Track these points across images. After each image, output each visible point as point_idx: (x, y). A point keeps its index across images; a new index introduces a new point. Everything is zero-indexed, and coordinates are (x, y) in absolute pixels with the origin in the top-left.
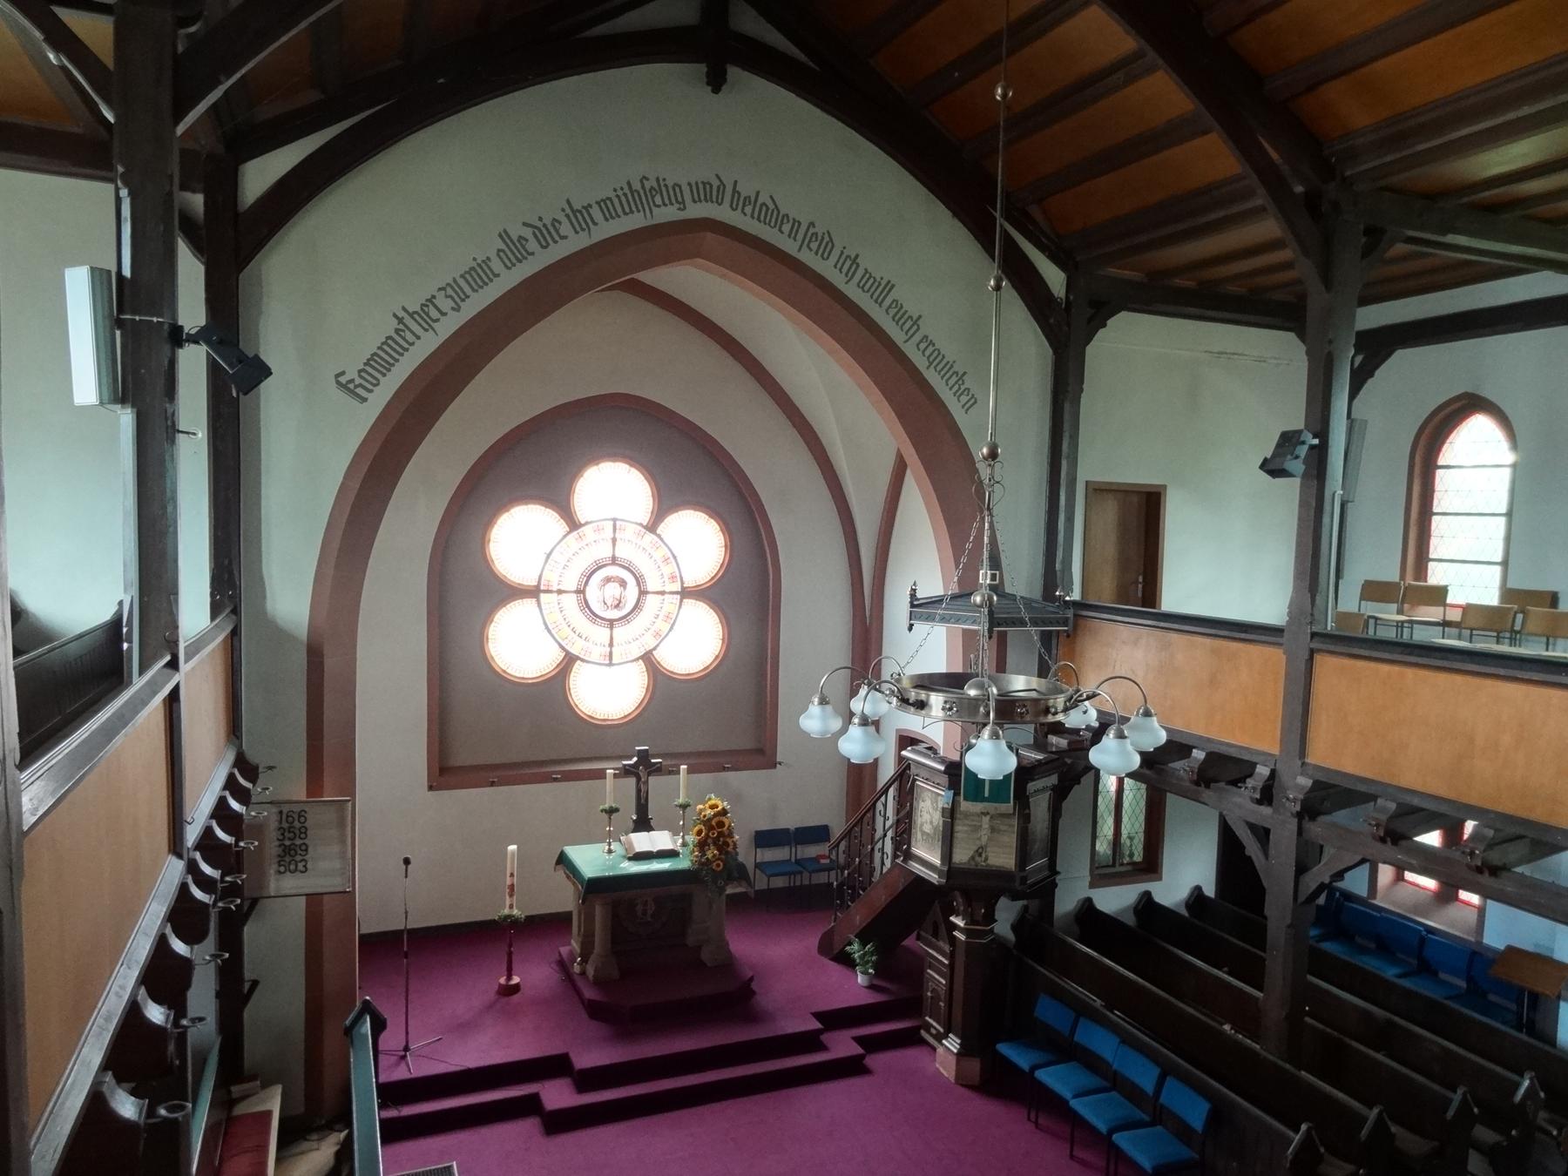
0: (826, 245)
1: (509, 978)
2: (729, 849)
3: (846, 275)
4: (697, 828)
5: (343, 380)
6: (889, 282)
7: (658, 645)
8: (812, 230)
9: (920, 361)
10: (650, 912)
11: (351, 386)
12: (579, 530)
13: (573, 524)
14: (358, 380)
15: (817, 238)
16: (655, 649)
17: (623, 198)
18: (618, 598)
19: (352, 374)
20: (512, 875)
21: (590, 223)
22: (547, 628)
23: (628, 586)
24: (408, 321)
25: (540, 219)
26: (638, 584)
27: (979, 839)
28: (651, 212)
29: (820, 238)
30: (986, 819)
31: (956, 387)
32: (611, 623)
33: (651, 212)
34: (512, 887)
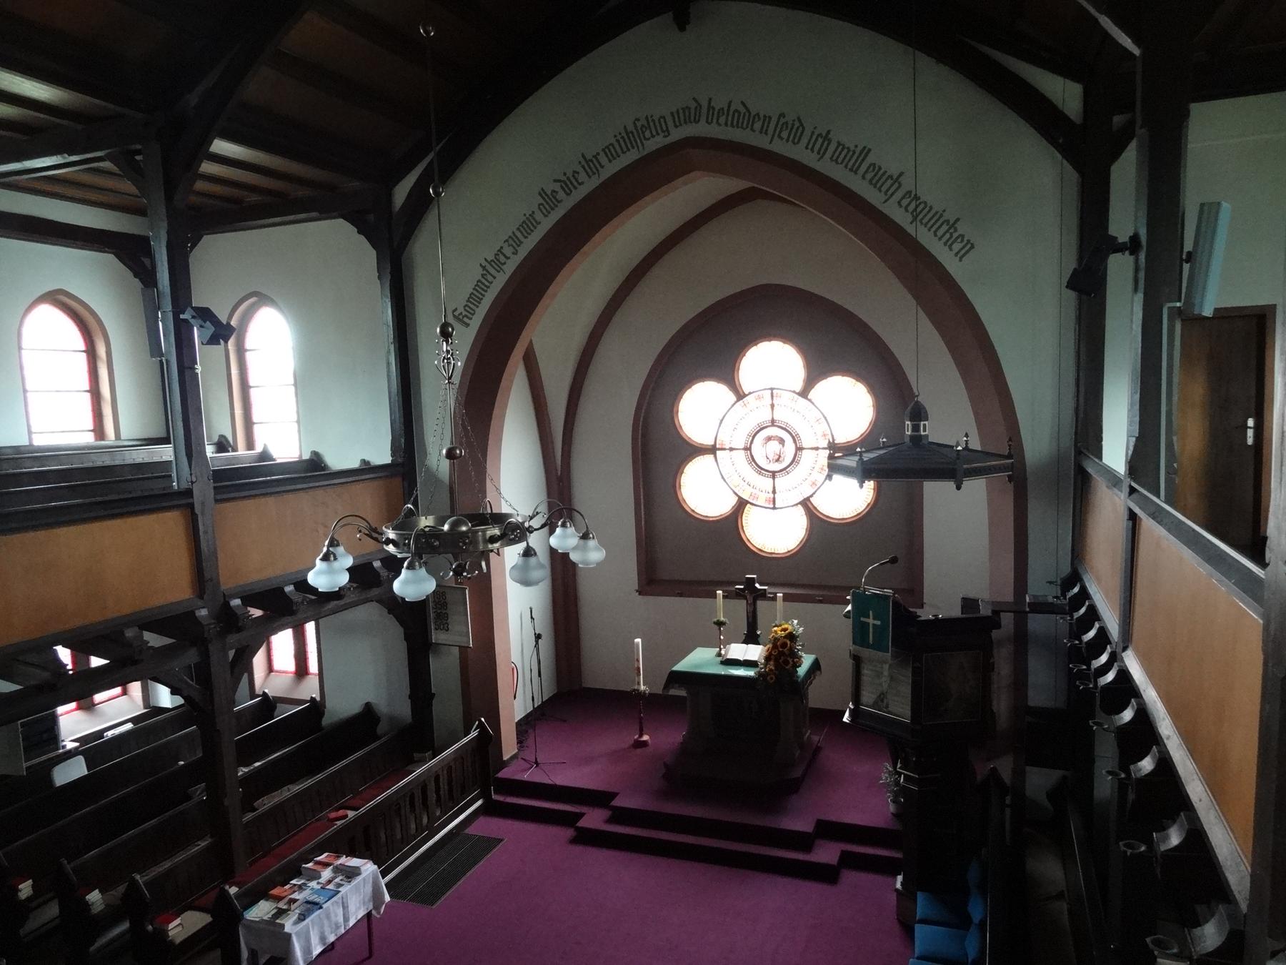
0: (795, 130)
1: (641, 736)
3: (818, 153)
5: (456, 313)
6: (865, 148)
7: (814, 493)
8: (782, 120)
9: (901, 217)
11: (461, 317)
12: (744, 400)
13: (740, 396)
14: (464, 313)
15: (787, 127)
16: (811, 496)
17: (621, 141)
18: (778, 453)
19: (461, 309)
21: (598, 166)
22: (723, 477)
23: (786, 444)
24: (489, 267)
25: (565, 174)
26: (795, 441)
27: (881, 684)
28: (643, 145)
29: (790, 126)
31: (948, 236)
32: (773, 474)
33: (643, 145)
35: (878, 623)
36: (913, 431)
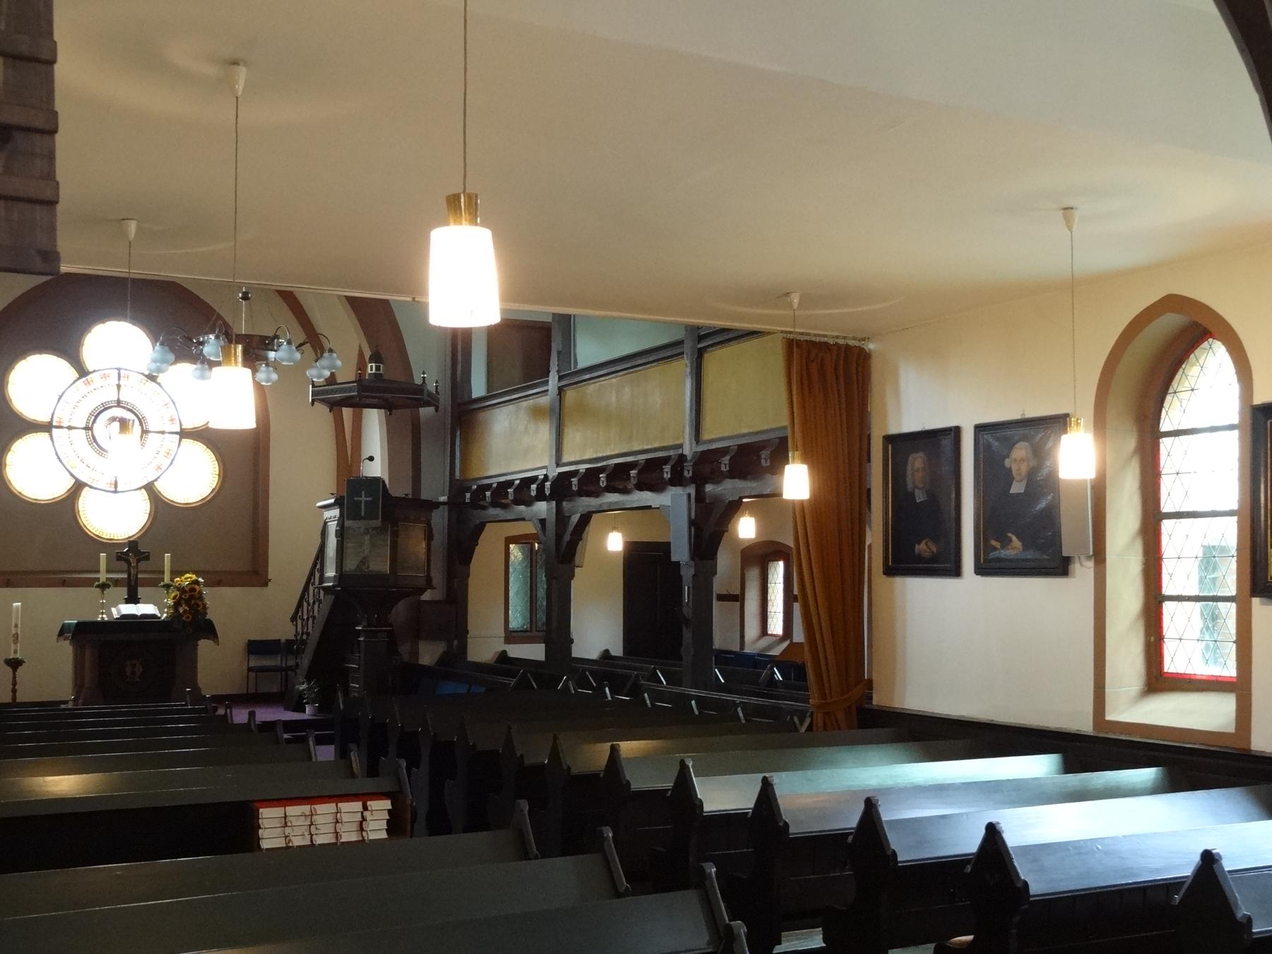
2: (199, 609)
4: (173, 594)
7: (159, 477)
10: (138, 673)
12: (88, 377)
13: (83, 372)
16: (156, 480)
20: (16, 626)
26: (141, 424)
30: (367, 537)
34: (16, 636)
35: (370, 499)
36: (376, 370)
